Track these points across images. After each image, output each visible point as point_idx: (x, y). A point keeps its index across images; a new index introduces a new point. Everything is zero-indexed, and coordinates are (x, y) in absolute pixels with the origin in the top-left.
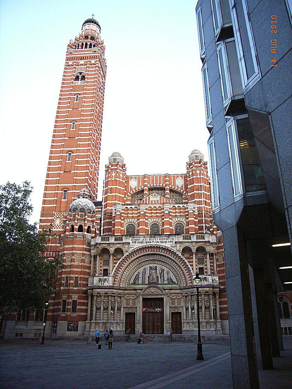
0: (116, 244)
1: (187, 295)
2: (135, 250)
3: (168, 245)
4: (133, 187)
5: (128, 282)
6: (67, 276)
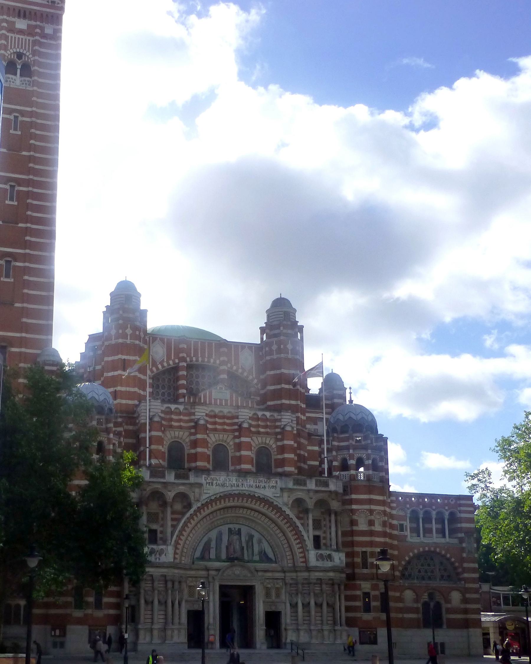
2: (213, 498)
3: (268, 493)
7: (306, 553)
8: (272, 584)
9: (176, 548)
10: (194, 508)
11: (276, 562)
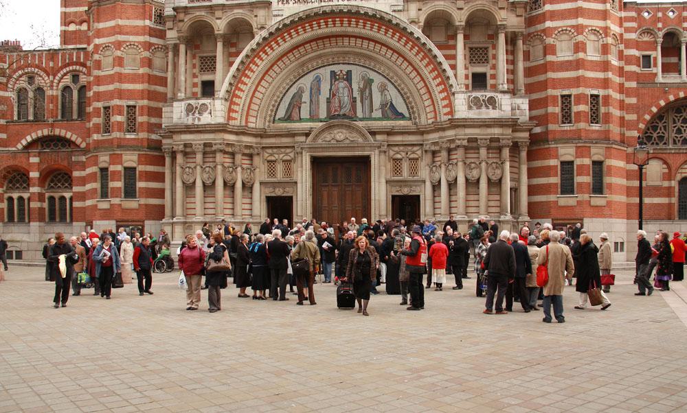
1: (437, 148)
2: (287, 22)
5: (270, 116)
6: (107, 105)
7: (452, 98)
8: (403, 154)
9: (232, 103)
10: (257, 39)
11: (410, 119)
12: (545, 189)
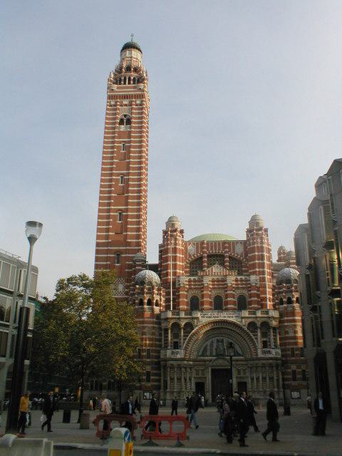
0: (186, 318)
3: (233, 320)
4: (192, 253)
12: (287, 380)
